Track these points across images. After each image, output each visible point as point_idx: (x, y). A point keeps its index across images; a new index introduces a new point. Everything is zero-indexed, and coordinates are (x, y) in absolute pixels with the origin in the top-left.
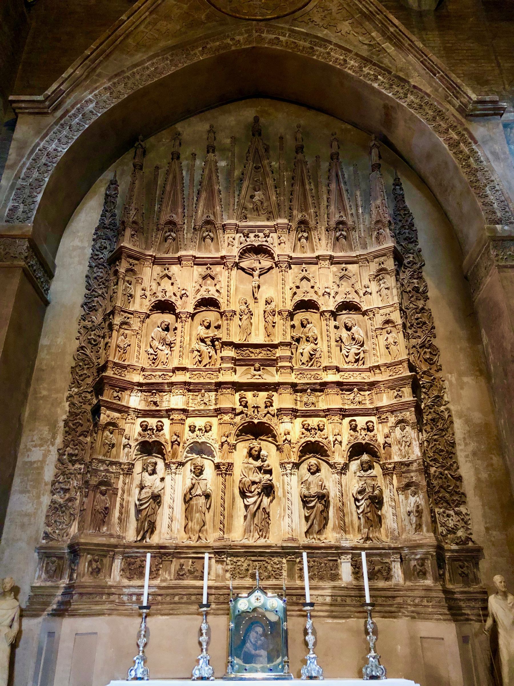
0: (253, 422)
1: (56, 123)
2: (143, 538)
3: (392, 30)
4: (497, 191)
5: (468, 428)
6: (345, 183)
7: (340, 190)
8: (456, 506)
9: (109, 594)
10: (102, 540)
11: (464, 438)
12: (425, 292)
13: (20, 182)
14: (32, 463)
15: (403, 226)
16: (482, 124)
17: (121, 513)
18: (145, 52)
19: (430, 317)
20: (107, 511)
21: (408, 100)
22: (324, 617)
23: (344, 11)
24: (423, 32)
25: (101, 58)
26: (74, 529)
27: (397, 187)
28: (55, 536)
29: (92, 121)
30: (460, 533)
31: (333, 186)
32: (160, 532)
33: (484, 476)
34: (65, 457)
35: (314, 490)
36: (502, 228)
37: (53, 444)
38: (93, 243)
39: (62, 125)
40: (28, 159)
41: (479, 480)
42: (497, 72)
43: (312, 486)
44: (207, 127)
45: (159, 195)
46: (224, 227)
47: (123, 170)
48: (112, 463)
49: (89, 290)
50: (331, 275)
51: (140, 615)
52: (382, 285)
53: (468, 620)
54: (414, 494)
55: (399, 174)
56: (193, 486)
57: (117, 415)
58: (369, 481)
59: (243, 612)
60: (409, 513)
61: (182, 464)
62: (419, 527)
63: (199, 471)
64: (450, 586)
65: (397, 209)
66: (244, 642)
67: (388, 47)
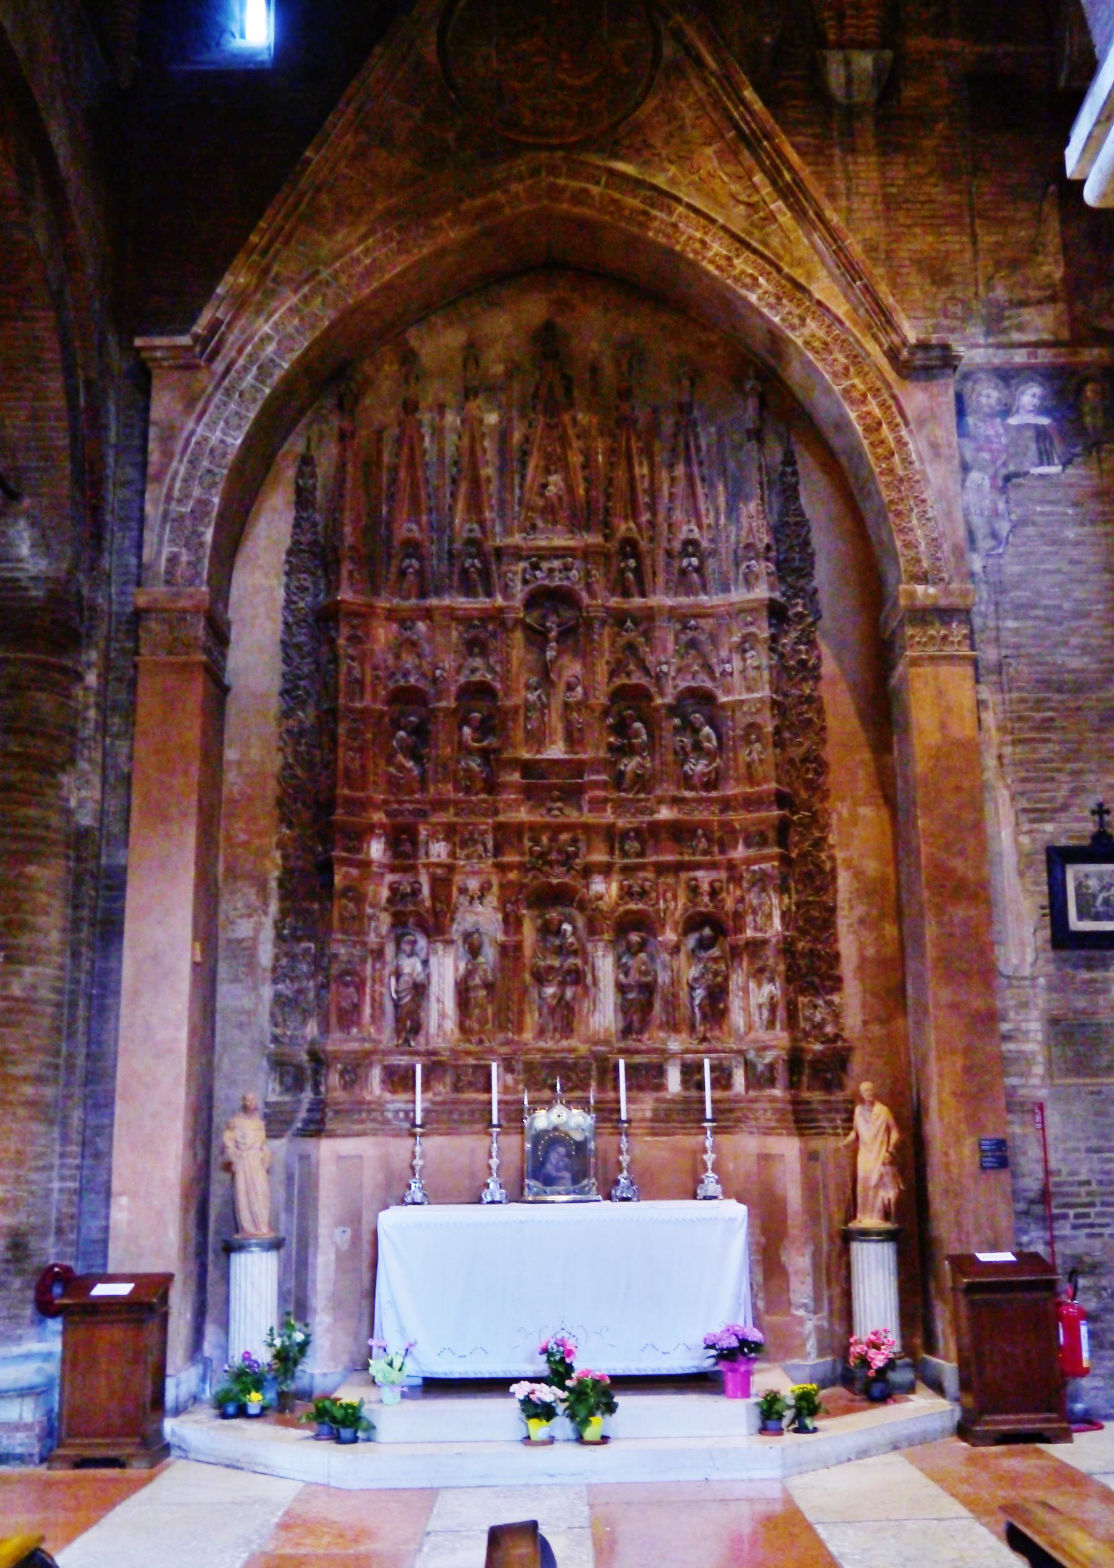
0: (550, 884)
1: (217, 387)
3: (788, 177)
4: (929, 519)
5: (856, 885)
6: (701, 463)
7: (690, 478)
9: (369, 1111)
10: (354, 1046)
11: (850, 900)
12: (816, 667)
13: (174, 506)
14: (240, 941)
16: (923, 384)
17: (373, 1007)
18: (353, 223)
19: (820, 711)
20: (357, 1007)
21: (806, 331)
23: (707, 123)
24: (850, 159)
25: (277, 245)
26: (312, 1029)
27: (789, 470)
28: (286, 1040)
30: (829, 1029)
31: (680, 470)
32: (427, 1033)
33: (870, 952)
34: (286, 932)
35: (634, 977)
37: (266, 913)
38: (284, 579)
40: (181, 461)
41: (863, 958)
42: (968, 256)
43: (632, 972)
46: (499, 552)
47: (321, 431)
48: (355, 944)
50: (671, 638)
51: (414, 1135)
52: (749, 662)
53: (823, 1133)
54: (771, 980)
55: (793, 439)
56: (470, 973)
57: (354, 872)
58: (710, 964)
60: (760, 1006)
61: (451, 942)
62: (771, 1024)
63: (474, 951)
64: (806, 1095)
65: (783, 513)
66: (543, 1164)
67: (780, 210)
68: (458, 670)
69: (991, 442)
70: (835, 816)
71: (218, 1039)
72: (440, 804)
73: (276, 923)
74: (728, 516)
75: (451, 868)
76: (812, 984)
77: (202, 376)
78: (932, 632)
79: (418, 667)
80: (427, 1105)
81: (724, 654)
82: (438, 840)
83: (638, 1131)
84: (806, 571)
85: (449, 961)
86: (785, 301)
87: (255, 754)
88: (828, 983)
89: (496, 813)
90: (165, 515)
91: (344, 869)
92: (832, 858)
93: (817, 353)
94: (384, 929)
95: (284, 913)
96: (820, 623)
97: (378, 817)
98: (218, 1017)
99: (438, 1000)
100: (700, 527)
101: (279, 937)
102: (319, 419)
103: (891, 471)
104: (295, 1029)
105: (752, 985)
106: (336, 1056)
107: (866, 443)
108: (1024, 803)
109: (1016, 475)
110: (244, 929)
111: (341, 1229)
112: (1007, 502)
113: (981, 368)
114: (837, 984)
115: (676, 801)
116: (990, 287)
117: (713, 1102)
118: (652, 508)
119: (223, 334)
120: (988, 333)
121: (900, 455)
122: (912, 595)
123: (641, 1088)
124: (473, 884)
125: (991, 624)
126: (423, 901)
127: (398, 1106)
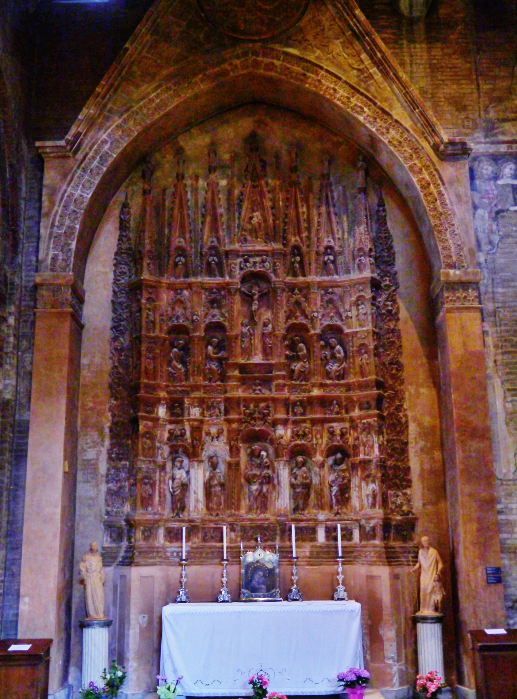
0: (255, 430)
1: (78, 167)
2: (178, 514)
3: (379, 55)
4: (456, 235)
7: (329, 214)
8: (403, 489)
9: (158, 552)
10: (150, 517)
11: (416, 438)
12: (397, 313)
13: (55, 229)
15: (383, 250)
16: (452, 163)
17: (160, 497)
18: (150, 82)
19: (399, 337)
20: (151, 496)
21: (390, 136)
22: (304, 565)
23: (336, 27)
24: (412, 46)
25: (110, 93)
26: (127, 508)
27: (381, 209)
28: (114, 514)
29: (109, 162)
30: (405, 508)
31: (323, 209)
32: (189, 510)
33: (427, 466)
34: (113, 456)
36: (454, 273)
37: (103, 446)
39: (83, 169)
41: (422, 470)
42: (475, 96)
43: (299, 477)
44: (207, 140)
45: (169, 219)
46: (227, 253)
48: (150, 462)
49: (115, 314)
50: (319, 298)
51: (181, 565)
52: (361, 311)
54: (374, 482)
55: (384, 192)
56: (211, 478)
57: (150, 424)
58: (340, 473)
59: (250, 563)
60: (368, 496)
61: (202, 461)
62: (373, 505)
63: (214, 466)
64: (392, 543)
65: (379, 232)
66: (251, 581)
67: (375, 73)
68: (206, 315)
69: (489, 194)
70: (407, 393)
71: (77, 513)
72: (196, 388)
73: (108, 450)
74: (349, 233)
75: (201, 422)
76: (395, 483)
77: (71, 162)
78: (458, 295)
79: (184, 315)
80: (188, 549)
81: (347, 307)
82: (195, 407)
83: (302, 563)
84: (391, 263)
85: (201, 472)
86: (378, 120)
87: (97, 360)
88: (404, 483)
89: (226, 392)
90: (51, 234)
91: (145, 422)
92: (406, 416)
93: (395, 147)
94: (166, 455)
95: (112, 445)
96: (398, 290)
97: (163, 394)
98: (77, 501)
99: (195, 493)
100: (334, 239)
101: (110, 459)
102: (131, 183)
103: (435, 209)
104: (118, 507)
105: (363, 484)
106: (140, 523)
107: (422, 194)
108: (508, 386)
109: (502, 211)
110: (91, 454)
111: (143, 615)
112: (497, 225)
113: (483, 155)
114: (409, 484)
115: (322, 386)
116: (487, 112)
117: (342, 547)
118: (309, 229)
119: (82, 140)
120: (486, 136)
121: (440, 200)
122: (448, 274)
123: (303, 540)
124: (214, 430)
125: (490, 290)
126: (186, 440)
127: (173, 549)
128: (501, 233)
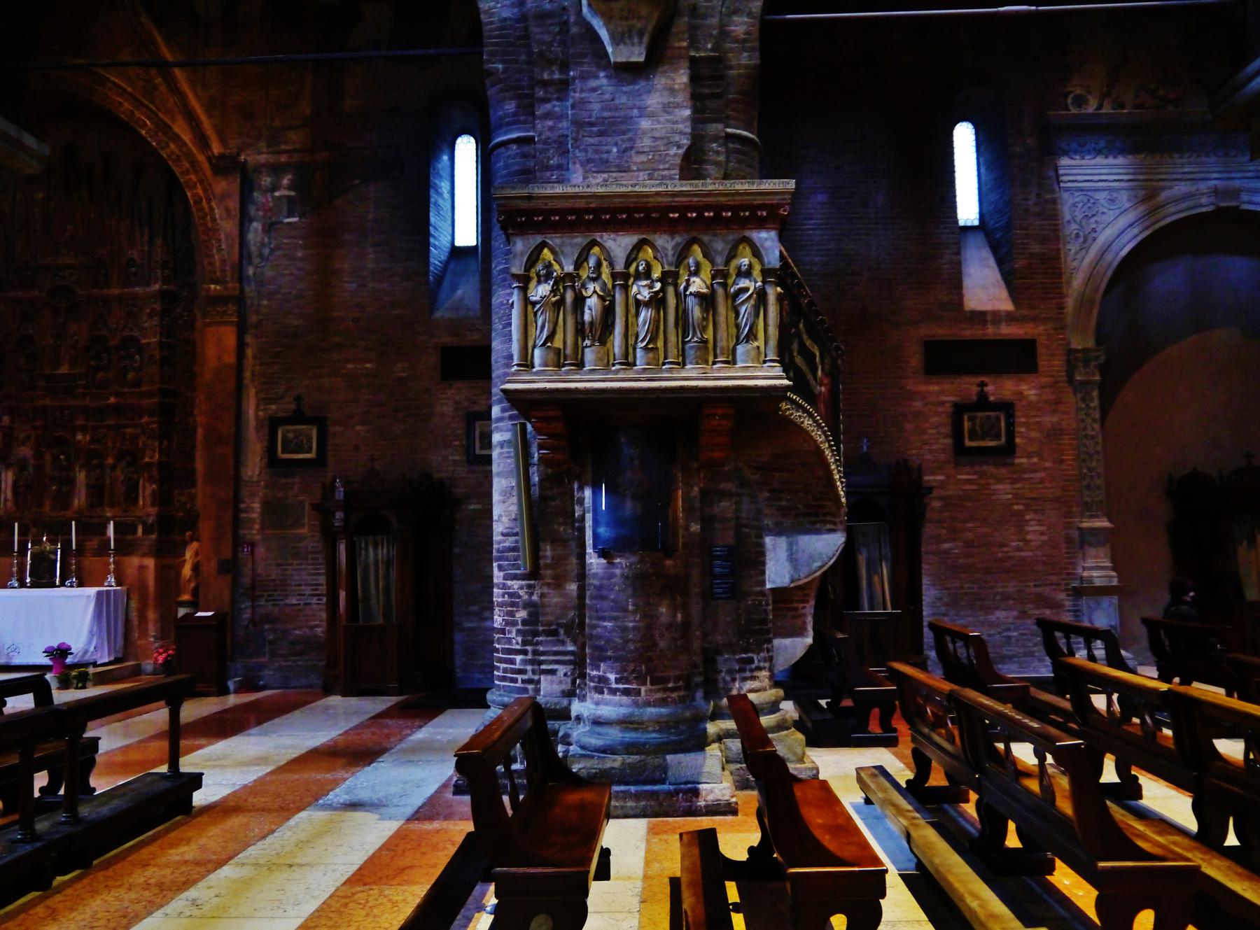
70: (198, 400)
78: (219, 309)
105: (147, 485)
108: (262, 395)
109: (276, 223)
113: (263, 165)
114: (193, 484)
115: (117, 394)
120: (268, 147)
122: (209, 289)
128: (272, 246)
